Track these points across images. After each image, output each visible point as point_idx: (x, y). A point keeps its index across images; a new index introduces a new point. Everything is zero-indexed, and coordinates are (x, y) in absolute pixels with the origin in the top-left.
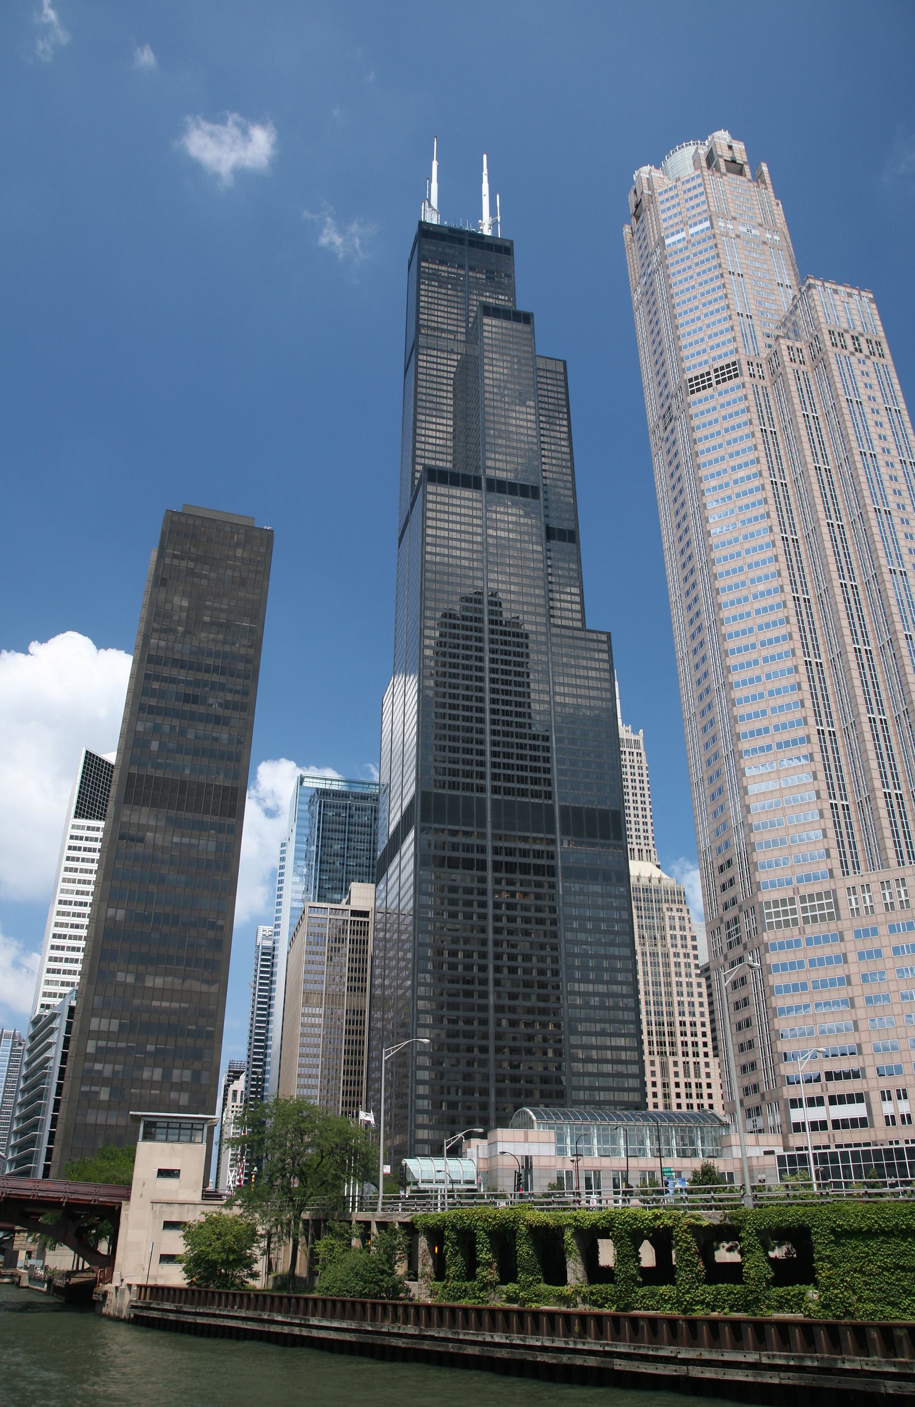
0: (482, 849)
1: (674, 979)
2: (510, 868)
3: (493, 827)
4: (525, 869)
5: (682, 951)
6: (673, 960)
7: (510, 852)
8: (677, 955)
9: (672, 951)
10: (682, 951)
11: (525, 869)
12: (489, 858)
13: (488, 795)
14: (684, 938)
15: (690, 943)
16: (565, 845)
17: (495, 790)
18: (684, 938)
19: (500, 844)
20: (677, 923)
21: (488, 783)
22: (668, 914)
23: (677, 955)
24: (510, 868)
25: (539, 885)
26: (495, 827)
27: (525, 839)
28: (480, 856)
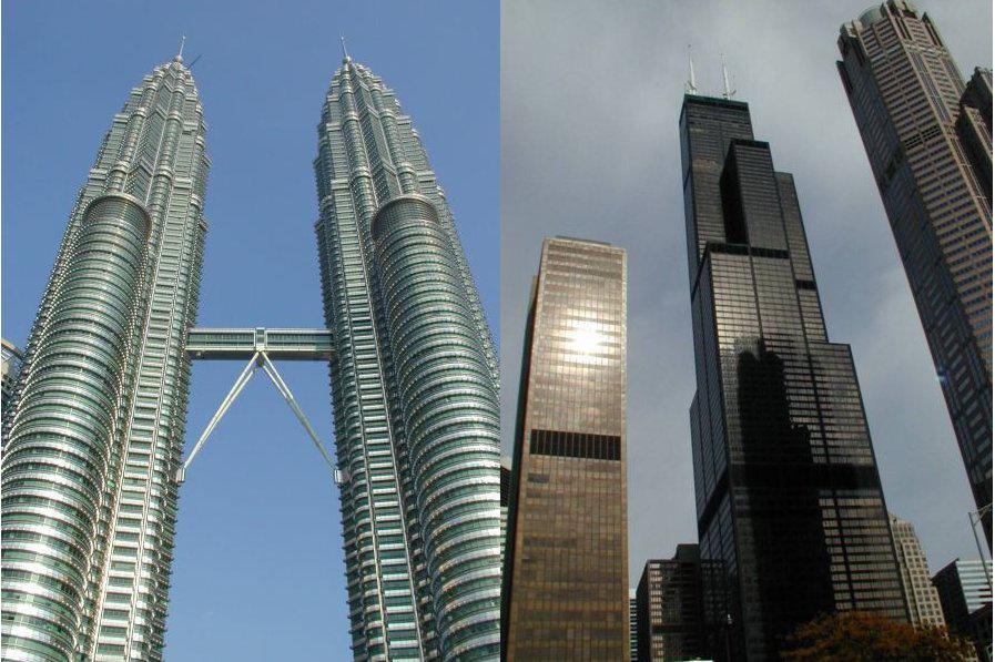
5: (917, 569)
6: (912, 576)
8: (915, 572)
9: (911, 570)
10: (917, 569)
14: (917, 560)
18: (917, 560)
20: (912, 551)
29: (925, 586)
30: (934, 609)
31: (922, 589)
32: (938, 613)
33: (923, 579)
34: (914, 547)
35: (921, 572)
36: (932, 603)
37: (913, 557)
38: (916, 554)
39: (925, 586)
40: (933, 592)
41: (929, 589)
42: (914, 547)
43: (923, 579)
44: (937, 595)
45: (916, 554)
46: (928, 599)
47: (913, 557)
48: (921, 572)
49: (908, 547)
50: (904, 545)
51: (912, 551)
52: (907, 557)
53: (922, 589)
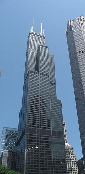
0: (38, 138)
1: (72, 164)
2: (43, 142)
3: (40, 134)
4: (46, 142)
5: (73, 159)
6: (71, 160)
7: (43, 139)
8: (72, 160)
10: (73, 159)
11: (46, 142)
12: (39, 140)
13: (39, 128)
15: (74, 157)
16: (53, 138)
17: (40, 127)
18: (73, 156)
19: (41, 137)
20: (72, 154)
21: (39, 126)
22: (70, 152)
23: (72, 160)
24: (43, 142)
25: (48, 145)
26: (40, 134)
27: (46, 137)
28: (38, 140)
29: (74, 163)
30: (76, 170)
31: (73, 164)
32: (77, 170)
33: (74, 161)
34: (73, 153)
35: (74, 160)
36: (76, 168)
37: (72, 156)
38: (73, 155)
39: (74, 163)
40: (76, 165)
41: (75, 164)
42: (73, 153)
43: (74, 161)
44: (77, 166)
45: (73, 155)
46: (75, 167)
47: (72, 156)
48: (74, 160)
49: (71, 153)
50: (70, 152)
51: (72, 154)
52: (71, 155)
53: (73, 164)
